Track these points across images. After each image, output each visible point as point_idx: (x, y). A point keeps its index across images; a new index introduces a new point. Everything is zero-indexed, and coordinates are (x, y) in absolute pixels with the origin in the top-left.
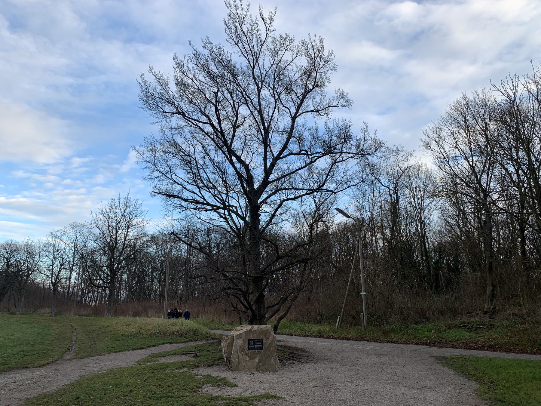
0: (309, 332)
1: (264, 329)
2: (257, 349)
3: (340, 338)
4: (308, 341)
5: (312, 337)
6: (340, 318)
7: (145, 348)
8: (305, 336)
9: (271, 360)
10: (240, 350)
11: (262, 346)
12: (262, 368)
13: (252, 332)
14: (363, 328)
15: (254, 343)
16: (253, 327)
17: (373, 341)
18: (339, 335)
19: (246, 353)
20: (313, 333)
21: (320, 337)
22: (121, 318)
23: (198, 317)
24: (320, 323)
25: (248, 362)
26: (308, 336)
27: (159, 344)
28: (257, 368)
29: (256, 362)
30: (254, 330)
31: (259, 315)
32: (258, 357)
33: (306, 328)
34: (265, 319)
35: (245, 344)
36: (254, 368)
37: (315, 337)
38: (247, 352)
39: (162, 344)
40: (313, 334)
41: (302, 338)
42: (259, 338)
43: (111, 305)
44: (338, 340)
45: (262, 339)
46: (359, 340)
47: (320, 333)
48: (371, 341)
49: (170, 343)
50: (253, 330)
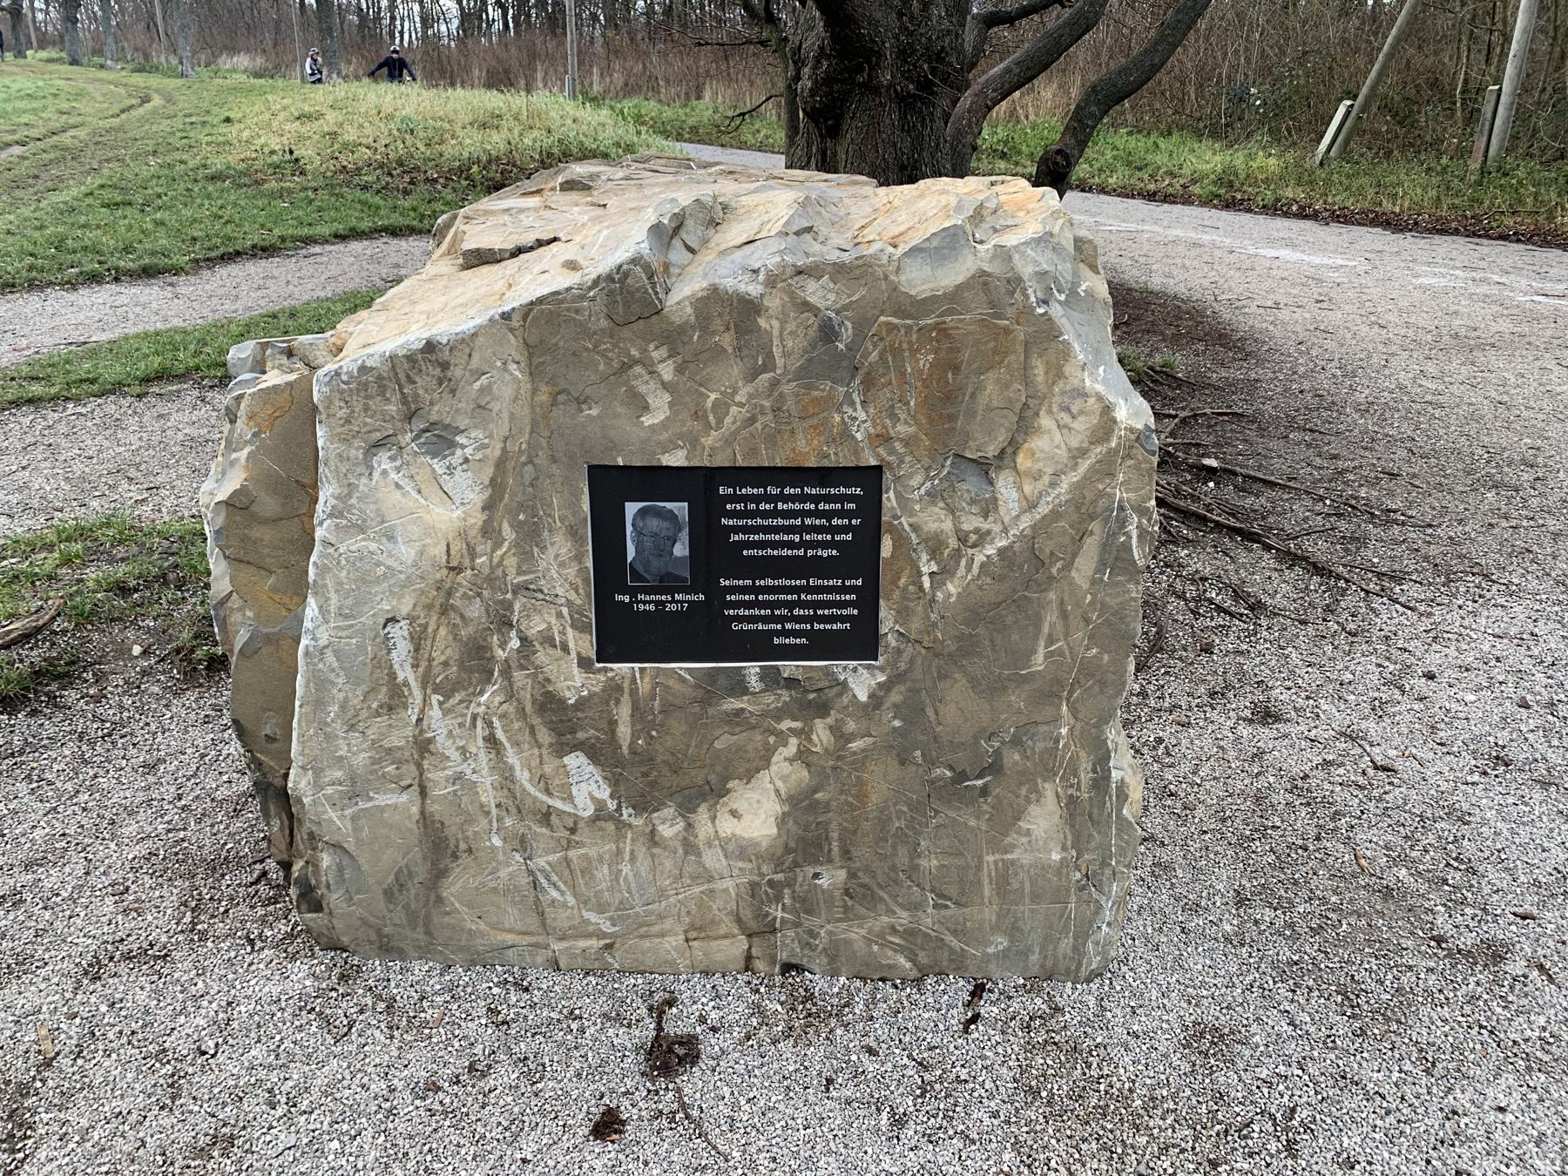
0: (1171, 174)
1: (921, 281)
2: (759, 647)
3: (1342, 217)
4: (1192, 235)
5: (1187, 200)
6: (1348, 113)
7: (177, 271)
8: (1151, 197)
9: (1008, 819)
10: (443, 648)
11: (869, 600)
12: (856, 934)
13: (673, 338)
14: (1475, 165)
15: (706, 531)
16: (714, 216)
17: (1546, 244)
18: (1338, 199)
19: (549, 703)
20: (1194, 182)
21: (1230, 205)
22: (460, 92)
23: (699, 98)
24: (1219, 131)
25: (592, 847)
26: (1168, 199)
27: (308, 241)
28: (760, 930)
29: (741, 850)
30: (714, 297)
31: (903, 54)
32: (783, 771)
33: (1160, 159)
34: (966, 101)
35: (526, 559)
36: (698, 930)
37: (1206, 202)
38: (573, 682)
39: (341, 237)
40: (1196, 189)
41: (1137, 204)
42: (806, 450)
43: (330, 30)
44: (1335, 228)
45: (871, 478)
46: (1456, 232)
47: (1231, 185)
48: (1529, 241)
49: (395, 232)
50: (684, 292)
